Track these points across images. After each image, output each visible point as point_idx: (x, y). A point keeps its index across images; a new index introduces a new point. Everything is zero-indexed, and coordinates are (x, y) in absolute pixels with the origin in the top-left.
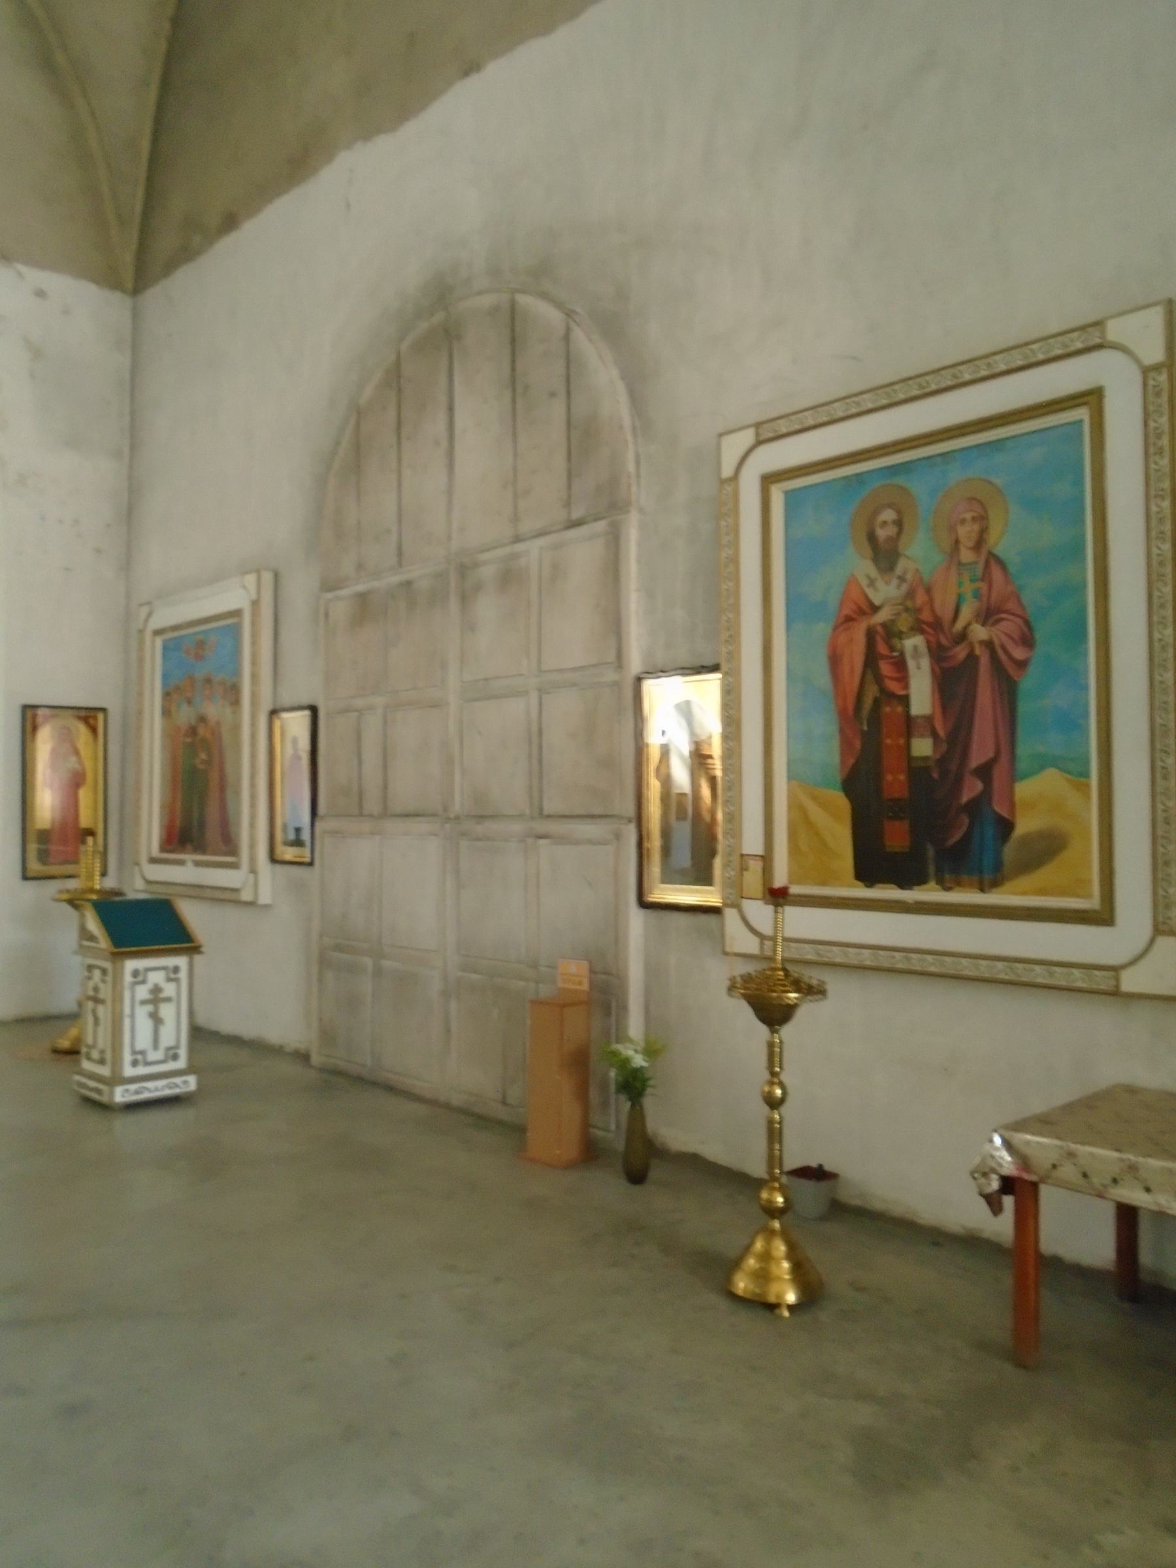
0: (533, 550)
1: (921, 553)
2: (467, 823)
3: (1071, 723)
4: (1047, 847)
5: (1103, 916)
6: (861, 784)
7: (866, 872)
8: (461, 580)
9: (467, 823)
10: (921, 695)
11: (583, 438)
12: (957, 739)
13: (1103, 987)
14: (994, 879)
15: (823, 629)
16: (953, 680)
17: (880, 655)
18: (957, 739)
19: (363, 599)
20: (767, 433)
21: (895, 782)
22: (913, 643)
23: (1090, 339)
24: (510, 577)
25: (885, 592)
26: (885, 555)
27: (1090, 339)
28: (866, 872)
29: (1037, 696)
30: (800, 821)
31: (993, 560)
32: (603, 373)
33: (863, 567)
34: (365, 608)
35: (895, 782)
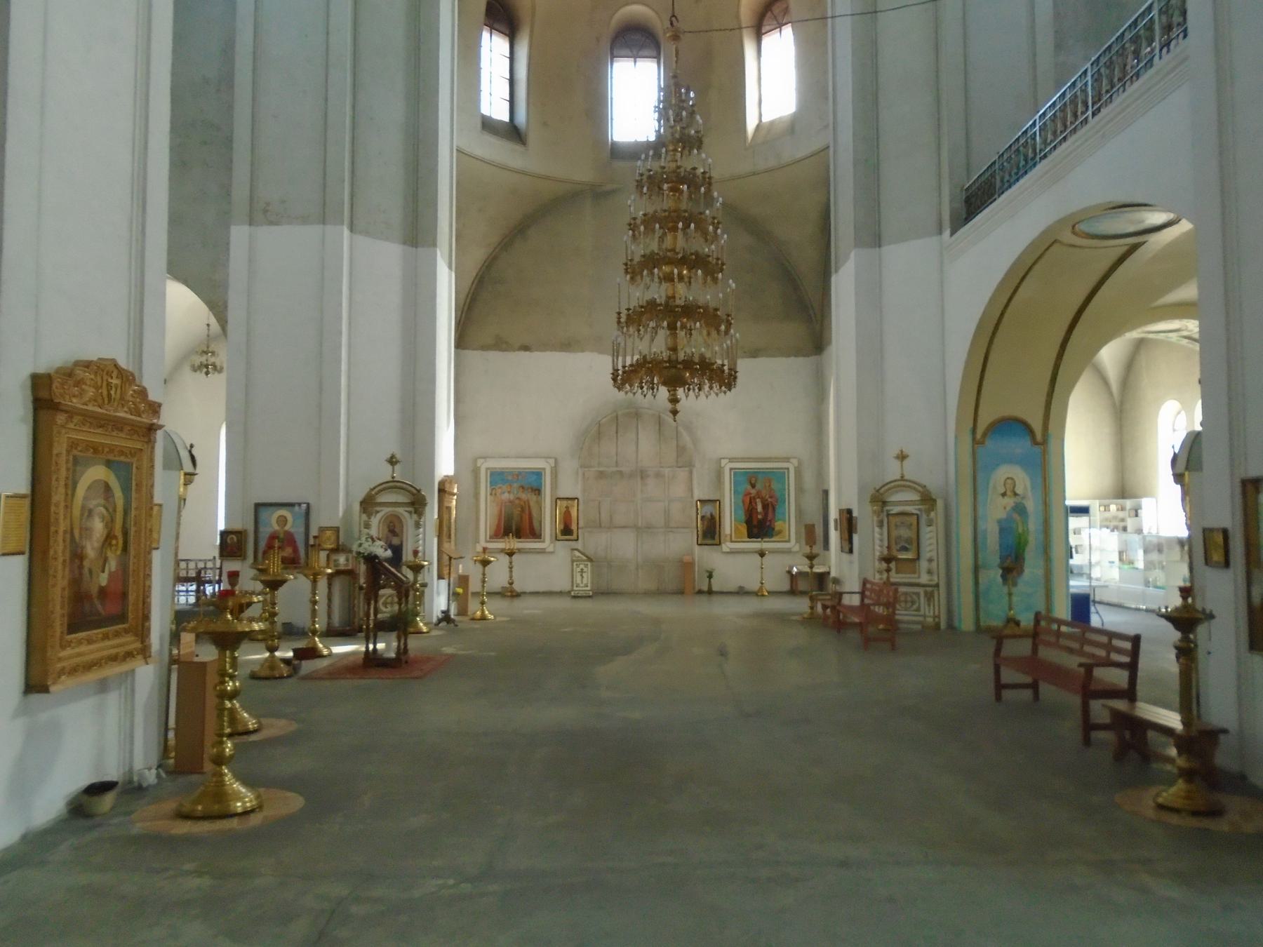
0: (667, 471)
1: (758, 486)
2: (643, 530)
3: (784, 514)
4: (780, 532)
5: (789, 541)
6: (749, 522)
7: (750, 536)
8: (643, 474)
9: (643, 530)
10: (760, 508)
11: (681, 450)
12: (766, 514)
13: (788, 552)
14: (772, 536)
15: (741, 497)
16: (765, 507)
17: (752, 501)
18: (766, 514)
19: (601, 473)
20: (732, 460)
21: (755, 523)
22: (758, 500)
23: (787, 460)
24: (658, 475)
25: (753, 492)
26: (753, 486)
27: (787, 460)
28: (750, 536)
29: (778, 510)
30: (737, 528)
31: (771, 490)
32: (686, 438)
33: (749, 487)
34: (601, 475)
35: (755, 523)
